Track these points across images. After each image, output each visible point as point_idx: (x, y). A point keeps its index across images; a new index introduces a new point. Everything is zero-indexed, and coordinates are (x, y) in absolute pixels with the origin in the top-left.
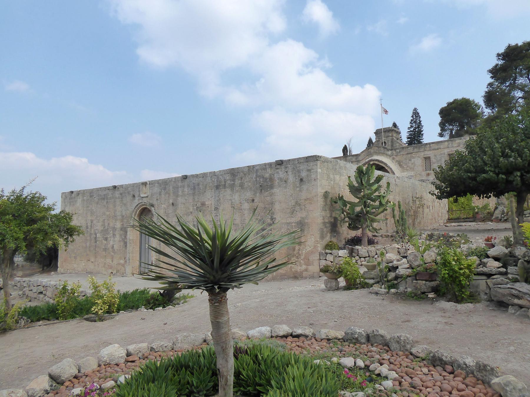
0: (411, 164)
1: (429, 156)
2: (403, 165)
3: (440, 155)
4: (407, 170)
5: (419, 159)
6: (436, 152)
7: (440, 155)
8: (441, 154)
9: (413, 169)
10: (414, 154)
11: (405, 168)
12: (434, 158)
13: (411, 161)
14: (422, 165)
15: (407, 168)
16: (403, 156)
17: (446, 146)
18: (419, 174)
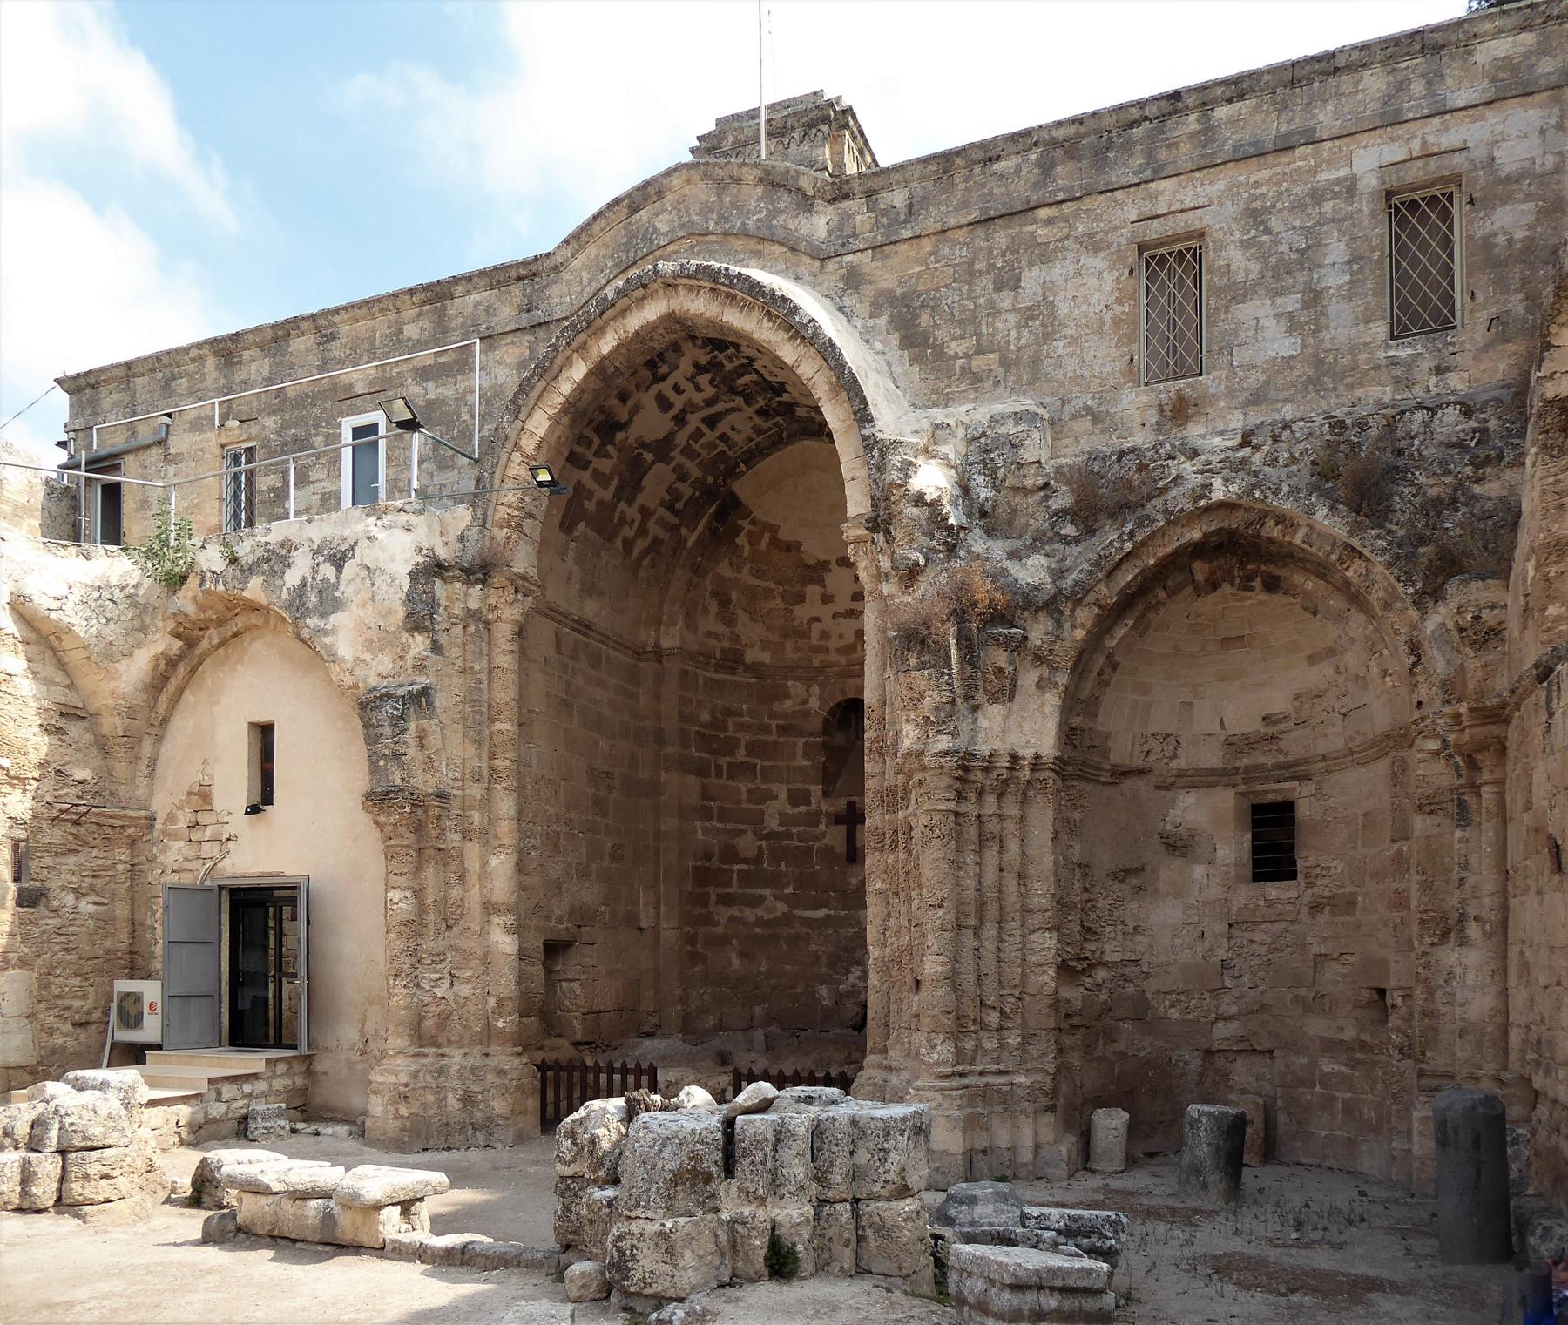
1: (1194, 221)
4: (976, 379)
9: (1035, 362)
14: (1117, 322)
15: (978, 363)
17: (1373, 107)
18: (1088, 410)
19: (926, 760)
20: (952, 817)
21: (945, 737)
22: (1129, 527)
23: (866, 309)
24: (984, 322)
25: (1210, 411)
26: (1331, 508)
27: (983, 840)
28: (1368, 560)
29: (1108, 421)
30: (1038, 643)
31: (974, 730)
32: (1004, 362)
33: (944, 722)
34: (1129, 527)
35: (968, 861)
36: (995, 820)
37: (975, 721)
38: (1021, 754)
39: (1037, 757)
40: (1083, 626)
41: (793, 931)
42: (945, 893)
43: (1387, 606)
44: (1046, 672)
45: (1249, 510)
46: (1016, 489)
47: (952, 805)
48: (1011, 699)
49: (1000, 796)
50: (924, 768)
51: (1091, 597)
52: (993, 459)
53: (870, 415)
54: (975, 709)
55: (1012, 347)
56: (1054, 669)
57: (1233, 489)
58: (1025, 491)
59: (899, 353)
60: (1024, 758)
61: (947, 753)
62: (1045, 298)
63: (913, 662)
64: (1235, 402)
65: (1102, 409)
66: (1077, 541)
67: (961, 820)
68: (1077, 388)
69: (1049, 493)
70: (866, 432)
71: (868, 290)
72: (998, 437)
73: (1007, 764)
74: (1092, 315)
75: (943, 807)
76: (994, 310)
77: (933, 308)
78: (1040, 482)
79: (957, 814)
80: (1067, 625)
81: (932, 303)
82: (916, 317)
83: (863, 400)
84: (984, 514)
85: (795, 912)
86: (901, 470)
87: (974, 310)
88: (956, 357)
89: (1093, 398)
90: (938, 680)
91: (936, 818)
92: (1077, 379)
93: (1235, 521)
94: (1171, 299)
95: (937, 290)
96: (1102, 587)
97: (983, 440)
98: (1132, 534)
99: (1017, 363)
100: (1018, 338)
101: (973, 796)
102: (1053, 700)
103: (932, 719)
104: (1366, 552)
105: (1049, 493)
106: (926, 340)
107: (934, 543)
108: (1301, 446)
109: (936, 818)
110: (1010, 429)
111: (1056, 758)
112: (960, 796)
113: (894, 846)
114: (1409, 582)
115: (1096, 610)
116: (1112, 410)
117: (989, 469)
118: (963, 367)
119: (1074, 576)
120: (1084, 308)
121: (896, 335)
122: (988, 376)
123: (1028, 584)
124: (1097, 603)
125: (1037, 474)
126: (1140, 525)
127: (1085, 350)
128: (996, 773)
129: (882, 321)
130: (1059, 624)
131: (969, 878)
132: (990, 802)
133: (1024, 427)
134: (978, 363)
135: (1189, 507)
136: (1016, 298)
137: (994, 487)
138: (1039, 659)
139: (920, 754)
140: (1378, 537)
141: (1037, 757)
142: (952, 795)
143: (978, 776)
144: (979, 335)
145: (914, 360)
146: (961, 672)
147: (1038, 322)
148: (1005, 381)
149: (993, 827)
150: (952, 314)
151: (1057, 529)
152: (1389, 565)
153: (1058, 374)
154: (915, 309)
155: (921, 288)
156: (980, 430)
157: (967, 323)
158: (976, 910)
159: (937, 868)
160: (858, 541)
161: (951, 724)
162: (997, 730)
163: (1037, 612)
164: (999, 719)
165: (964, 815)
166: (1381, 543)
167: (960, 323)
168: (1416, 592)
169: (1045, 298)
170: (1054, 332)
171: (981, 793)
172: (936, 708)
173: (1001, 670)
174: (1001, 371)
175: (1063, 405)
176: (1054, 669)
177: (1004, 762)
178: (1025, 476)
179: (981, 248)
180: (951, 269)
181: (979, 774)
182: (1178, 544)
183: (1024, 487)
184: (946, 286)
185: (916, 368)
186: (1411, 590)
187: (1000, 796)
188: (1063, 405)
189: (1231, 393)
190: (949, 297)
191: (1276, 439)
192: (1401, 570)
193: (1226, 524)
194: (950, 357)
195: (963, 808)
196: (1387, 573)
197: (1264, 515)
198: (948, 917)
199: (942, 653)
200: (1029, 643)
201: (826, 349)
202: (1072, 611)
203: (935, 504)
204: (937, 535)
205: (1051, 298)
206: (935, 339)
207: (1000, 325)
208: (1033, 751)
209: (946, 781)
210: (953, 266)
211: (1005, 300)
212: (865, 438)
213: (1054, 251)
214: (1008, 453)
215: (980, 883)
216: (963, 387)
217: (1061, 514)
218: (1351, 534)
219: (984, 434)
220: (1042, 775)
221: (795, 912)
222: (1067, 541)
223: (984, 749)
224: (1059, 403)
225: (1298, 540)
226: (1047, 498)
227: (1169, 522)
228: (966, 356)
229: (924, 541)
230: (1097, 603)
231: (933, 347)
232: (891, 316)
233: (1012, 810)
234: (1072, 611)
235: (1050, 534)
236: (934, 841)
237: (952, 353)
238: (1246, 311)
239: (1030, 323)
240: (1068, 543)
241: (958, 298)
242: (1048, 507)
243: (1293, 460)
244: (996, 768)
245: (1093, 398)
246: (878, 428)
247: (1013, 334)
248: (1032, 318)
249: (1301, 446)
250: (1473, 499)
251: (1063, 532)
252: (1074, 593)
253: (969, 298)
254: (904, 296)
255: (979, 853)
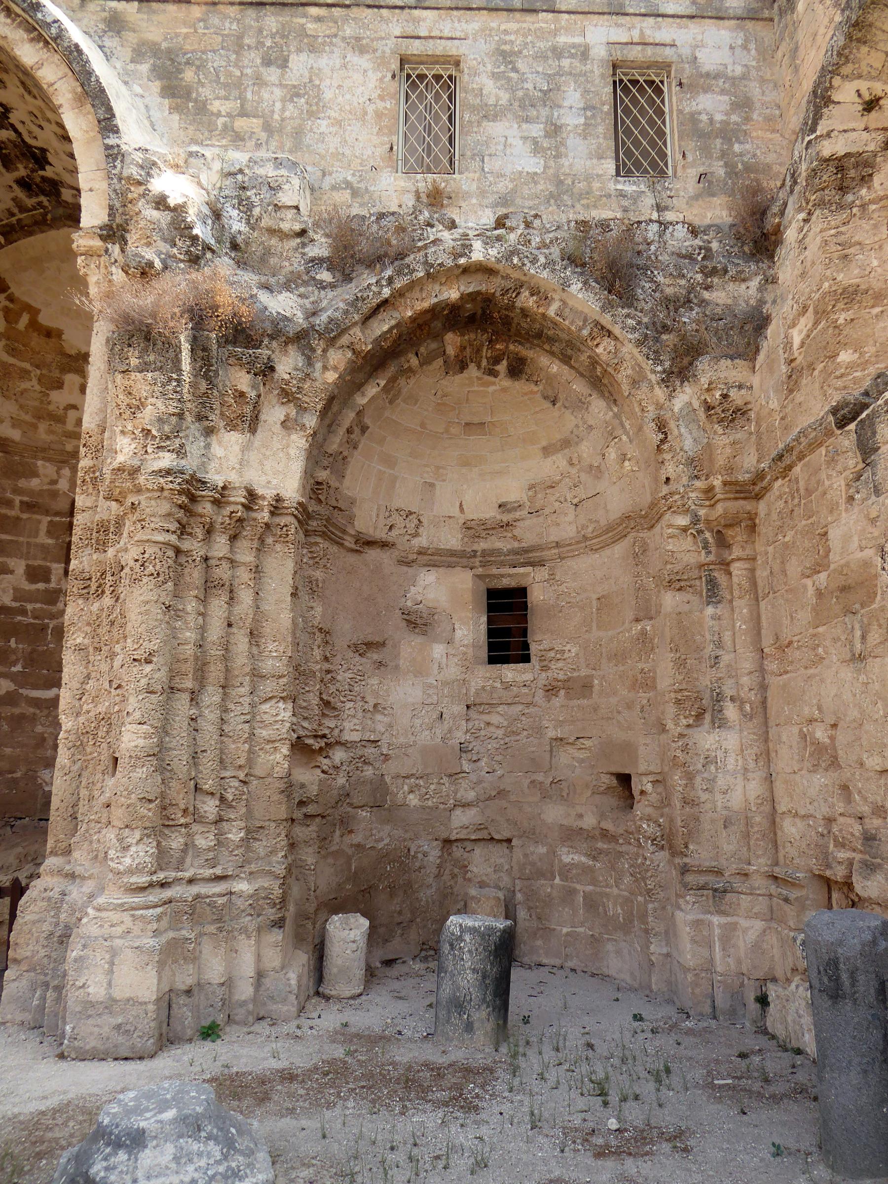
0: (278, 93)
2: (205, 92)
3: (541, 57)
5: (363, 62)
6: (512, 26)
7: (541, 57)
8: (558, 53)
9: (298, 134)
10: (319, 19)
11: (220, 121)
12: (495, 76)
13: (284, 64)
15: (241, 124)
16: (215, 20)
18: (348, 185)
19: (141, 479)
20: (171, 553)
21: (168, 455)
22: (389, 272)
23: (127, 53)
24: (250, 89)
25: (463, 204)
26: (585, 283)
27: (209, 586)
28: (616, 339)
29: (366, 197)
30: (287, 377)
31: (206, 456)
32: (267, 127)
33: (168, 438)
34: (389, 272)
35: (189, 608)
36: (225, 565)
37: (208, 446)
38: (260, 492)
39: (278, 499)
40: (335, 368)
41: (17, 711)
42: (154, 645)
43: (635, 383)
44: (293, 413)
45: (507, 277)
46: (272, 232)
47: (173, 538)
48: (253, 430)
49: (234, 538)
50: (139, 490)
51: (345, 340)
52: (249, 198)
53: (116, 126)
54: (209, 432)
55: (276, 117)
56: (302, 409)
57: (493, 252)
58: (282, 235)
59: (159, 100)
60: (263, 498)
61: (169, 472)
62: (311, 81)
63: (134, 362)
64: (486, 202)
65: (362, 185)
66: (332, 286)
67: (183, 559)
68: (338, 164)
69: (306, 241)
70: (111, 141)
71: (131, 38)
72: (255, 177)
73: (243, 500)
74: (356, 104)
75: (160, 537)
76: (259, 81)
77: (198, 68)
78: (297, 227)
79: (178, 551)
80: (319, 365)
81: (198, 63)
82: (180, 71)
83: (109, 109)
84: (235, 246)
85: (21, 691)
86: (142, 167)
87: (240, 78)
88: (219, 114)
89: (354, 175)
90: (163, 385)
91: (151, 550)
92: (338, 156)
93: (491, 286)
94: (429, 108)
95: (203, 52)
96: (357, 331)
97: (239, 177)
98: (390, 280)
99: (280, 130)
100: (283, 109)
101: (199, 532)
102: (298, 443)
103: (154, 432)
104: (617, 330)
105: (306, 241)
106: (189, 93)
107: (175, 250)
108: (551, 235)
109: (151, 550)
110: (269, 171)
111: (299, 504)
112: (183, 530)
113: (100, 593)
114: (657, 361)
115: (349, 354)
116: (372, 188)
117: (245, 206)
118: (225, 125)
119: (329, 313)
120: (348, 96)
121: (158, 83)
122: (250, 138)
123: (278, 313)
124: (351, 347)
125: (295, 220)
126: (399, 272)
127: (347, 133)
128: (230, 509)
129: (144, 68)
130: (309, 361)
131: (189, 629)
132: (220, 546)
133: (283, 172)
134: (241, 124)
135: (449, 263)
136: (283, 75)
137: (248, 222)
138: (287, 396)
139: (134, 472)
140: (628, 316)
141: (278, 499)
142: (173, 526)
143: (206, 508)
144: (242, 98)
145: (174, 109)
146: (194, 385)
147: (303, 100)
148: (267, 143)
149: (222, 572)
150: (217, 76)
151: (312, 274)
152: (640, 343)
153: (321, 148)
154: (180, 64)
155: (188, 47)
156: (238, 167)
157: (234, 87)
158: (196, 671)
159: (147, 612)
160: (89, 254)
161: (177, 441)
162: (233, 461)
163: (286, 344)
164: (237, 448)
165: (187, 553)
166: (631, 322)
167: (226, 86)
168: (664, 371)
169: (311, 81)
170: (318, 111)
171: (209, 531)
172: (160, 420)
173: (242, 394)
174: (263, 136)
175: (324, 175)
176: (302, 409)
177: (239, 497)
178: (282, 219)
179: (251, 27)
180: (220, 38)
181: (208, 506)
182: (436, 300)
183: (280, 231)
184: (214, 51)
185: (176, 117)
186: (659, 368)
187: (234, 538)
188: (324, 175)
189: (482, 193)
190: (216, 61)
191: (528, 225)
192: (649, 348)
193: (483, 288)
194: (212, 114)
195: (185, 545)
196: (635, 351)
197: (519, 286)
198: (157, 675)
199: (171, 354)
200: (276, 376)
201: (71, 52)
202: (325, 351)
203: (178, 211)
204: (179, 243)
205: (317, 82)
206: (198, 94)
207: (265, 95)
208: (275, 492)
209: (165, 507)
210: (222, 35)
211: (272, 74)
212: (108, 147)
213: (324, 44)
214: (265, 194)
215: (203, 638)
216: (224, 142)
217: (317, 262)
218: (603, 309)
219: (241, 171)
220: (283, 521)
221: (21, 691)
222: (322, 286)
223: (217, 478)
224: (320, 174)
225: (552, 312)
226: (304, 245)
227: (428, 275)
228: (229, 115)
229: (164, 247)
230: (351, 347)
231: (196, 101)
232: (154, 65)
233: (245, 554)
234: (325, 351)
235: (305, 278)
236: (145, 580)
237: (215, 111)
238: (498, 129)
239: (295, 100)
240: (324, 288)
241: (224, 64)
242: (304, 254)
243: (543, 245)
244: (229, 503)
245: (354, 175)
246: (123, 140)
247: (278, 105)
248: (298, 95)
249: (551, 235)
250: (703, 303)
251: (318, 277)
252: (328, 330)
253: (236, 66)
254: (169, 51)
255: (204, 601)
